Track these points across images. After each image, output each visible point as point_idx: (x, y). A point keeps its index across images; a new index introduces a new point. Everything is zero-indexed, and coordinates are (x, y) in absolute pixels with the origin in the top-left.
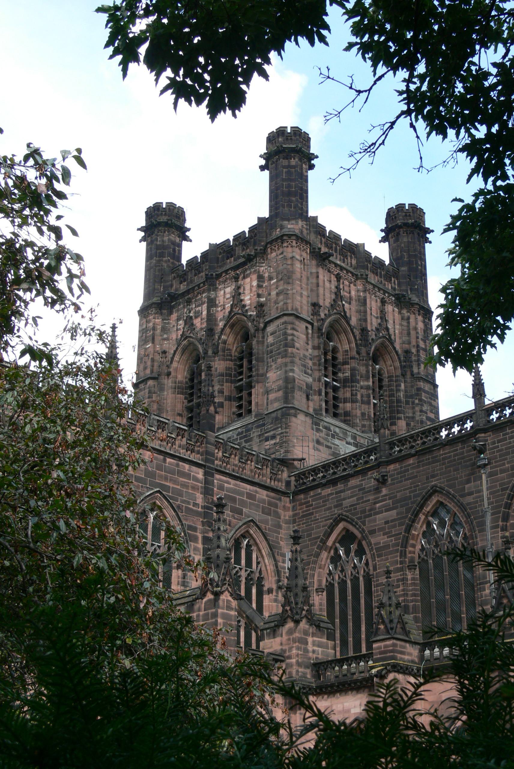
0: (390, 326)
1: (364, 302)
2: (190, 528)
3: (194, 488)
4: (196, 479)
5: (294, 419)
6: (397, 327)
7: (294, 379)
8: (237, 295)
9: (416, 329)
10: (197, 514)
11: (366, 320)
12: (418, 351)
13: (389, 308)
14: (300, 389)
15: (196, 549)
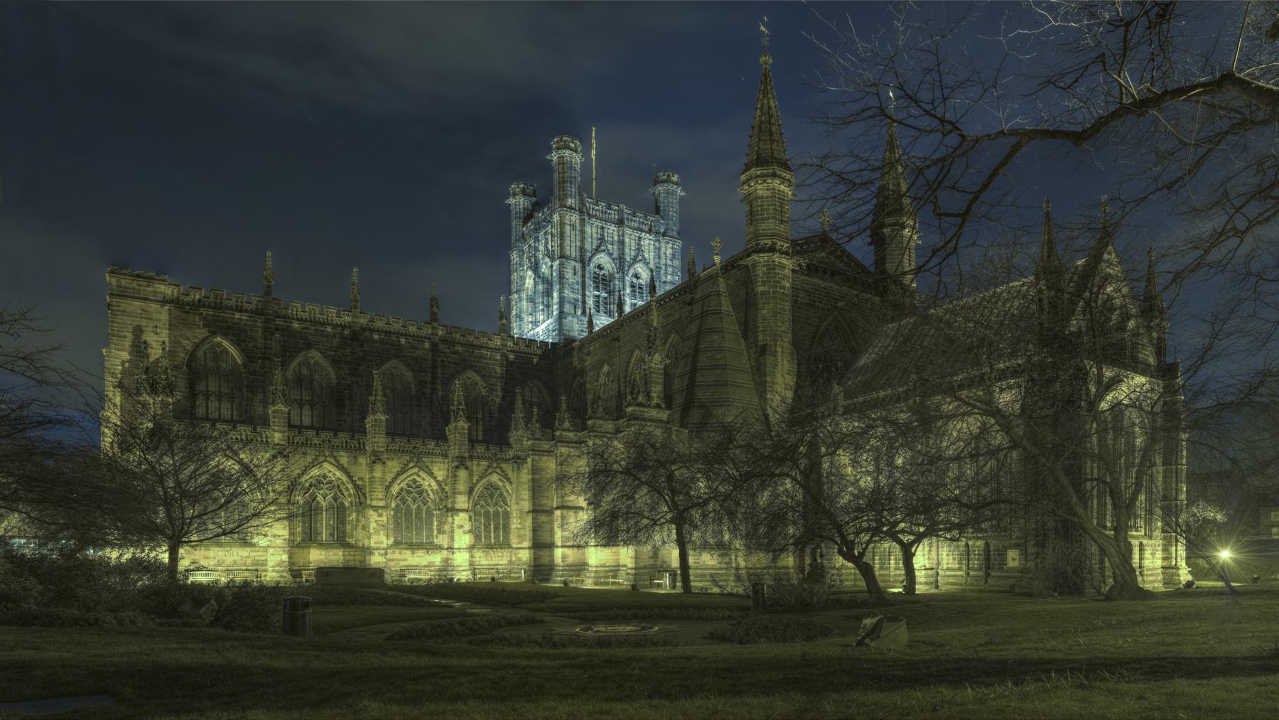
0: (646, 256)
1: (622, 243)
2: (492, 385)
3: (493, 365)
4: (496, 360)
5: (564, 320)
6: (652, 254)
7: (564, 297)
8: (547, 243)
9: (665, 253)
10: (496, 377)
11: (623, 254)
12: (666, 268)
13: (645, 243)
14: (569, 302)
15: (497, 396)
